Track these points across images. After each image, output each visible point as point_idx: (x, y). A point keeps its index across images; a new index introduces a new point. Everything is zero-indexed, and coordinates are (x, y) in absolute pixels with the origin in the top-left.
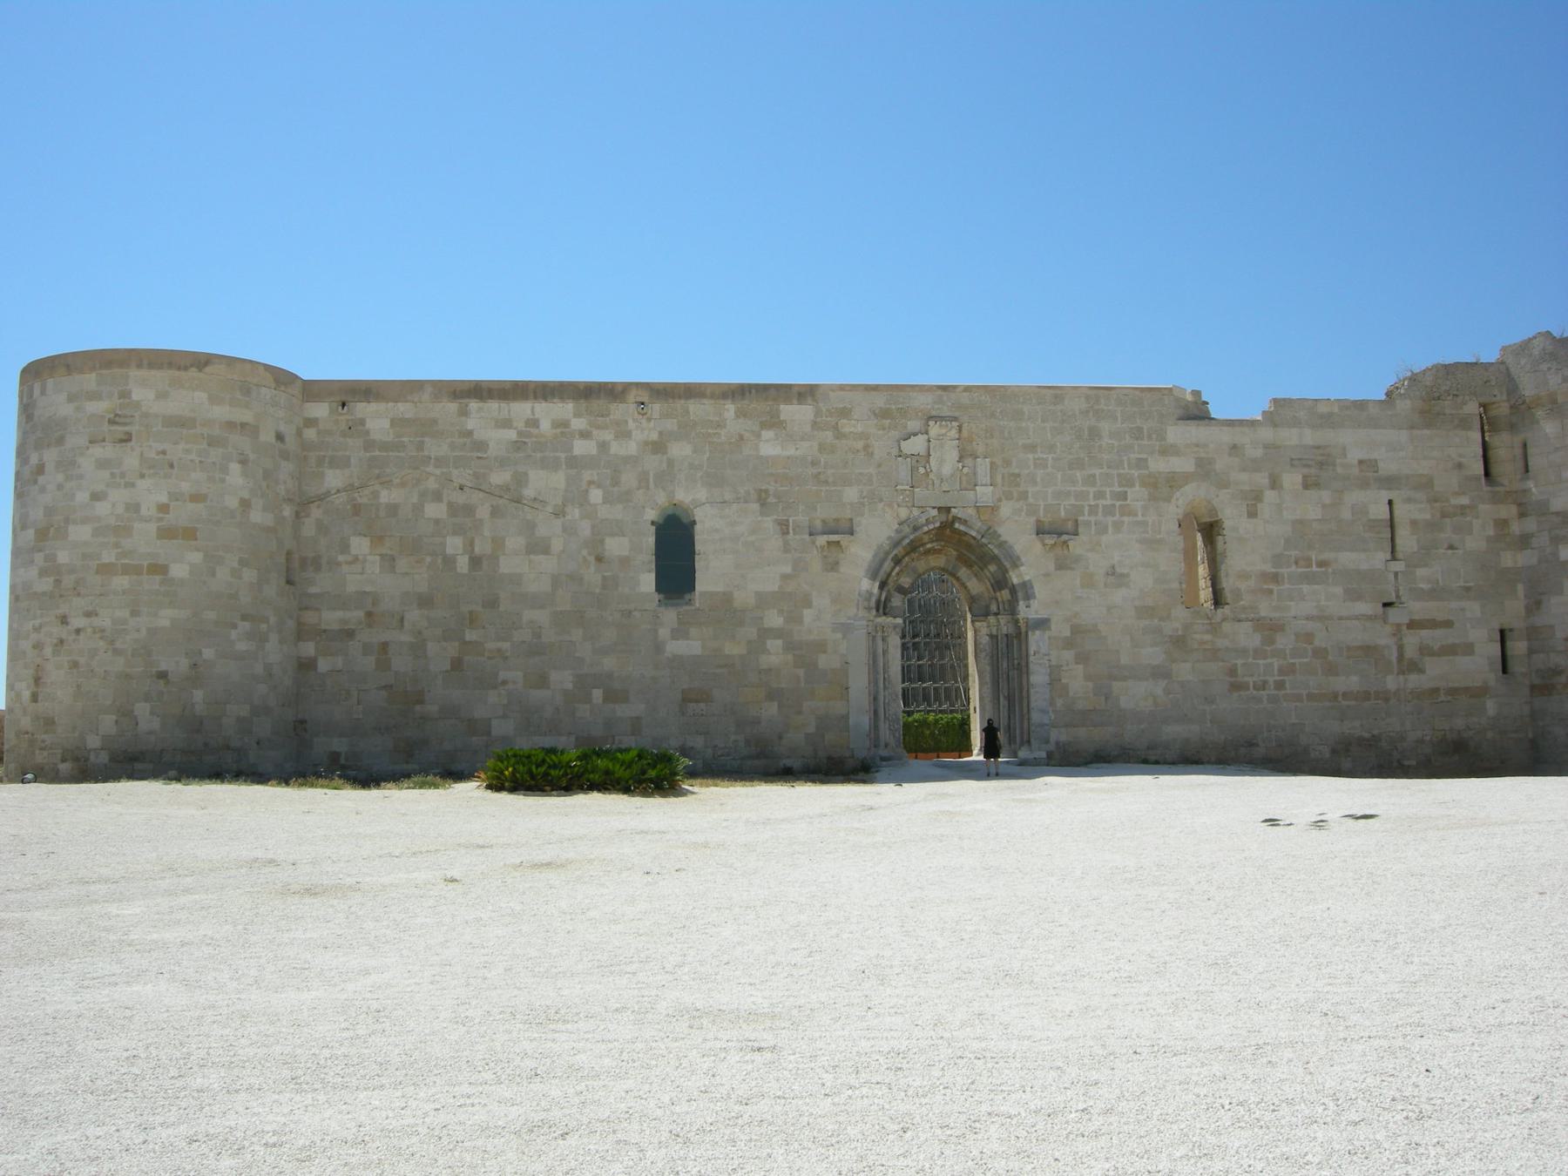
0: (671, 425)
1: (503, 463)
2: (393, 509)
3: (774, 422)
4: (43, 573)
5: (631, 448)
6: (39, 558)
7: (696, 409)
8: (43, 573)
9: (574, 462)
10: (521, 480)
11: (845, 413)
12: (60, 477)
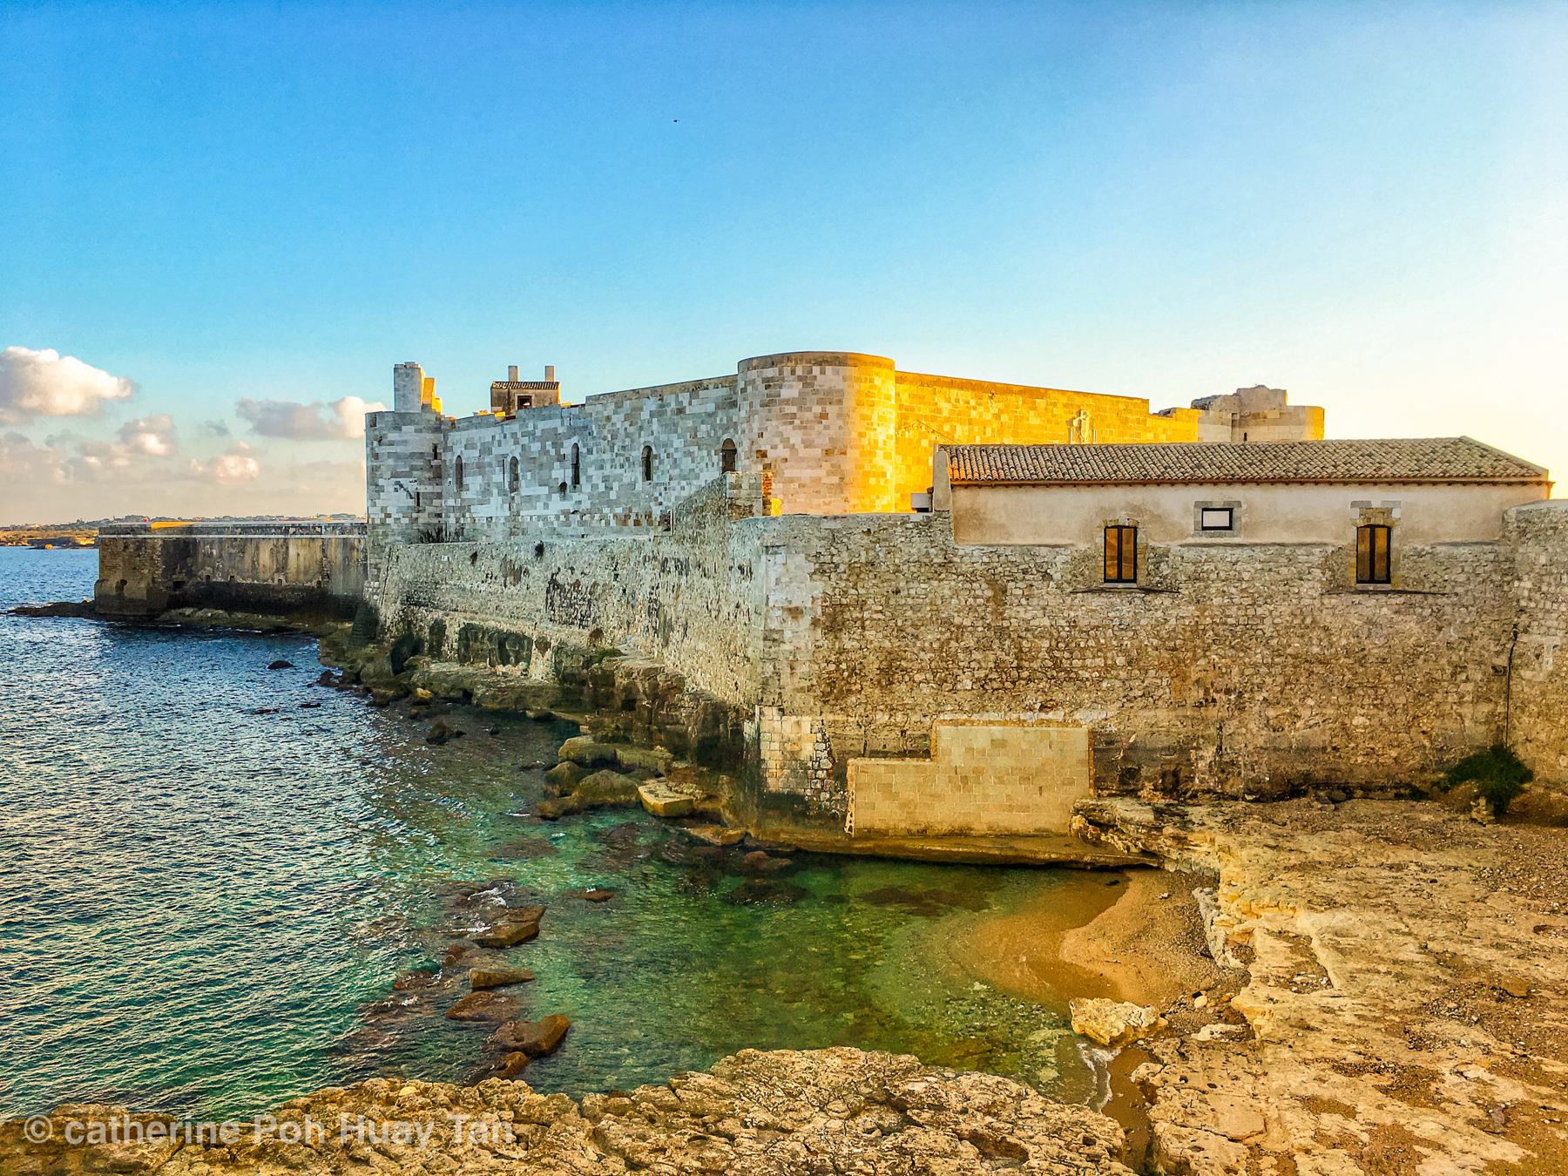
0: (1001, 405)
1: (948, 420)
2: (910, 440)
3: (1034, 408)
4: (829, 474)
5: (988, 416)
6: (827, 466)
7: (1012, 398)
8: (829, 474)
9: (971, 422)
10: (954, 429)
11: (1055, 404)
12: (840, 423)
